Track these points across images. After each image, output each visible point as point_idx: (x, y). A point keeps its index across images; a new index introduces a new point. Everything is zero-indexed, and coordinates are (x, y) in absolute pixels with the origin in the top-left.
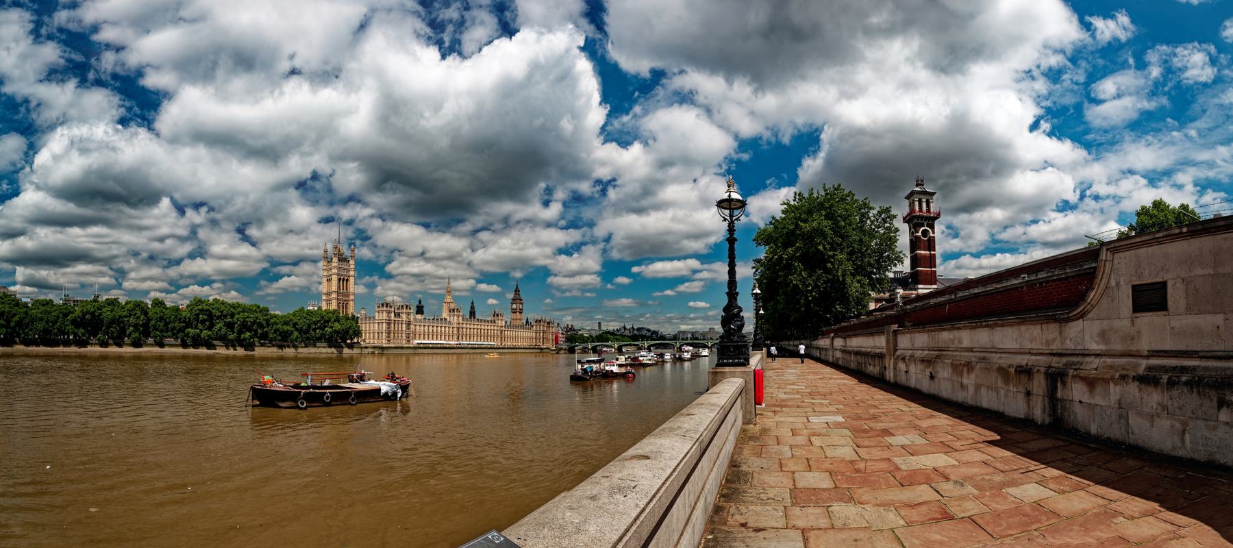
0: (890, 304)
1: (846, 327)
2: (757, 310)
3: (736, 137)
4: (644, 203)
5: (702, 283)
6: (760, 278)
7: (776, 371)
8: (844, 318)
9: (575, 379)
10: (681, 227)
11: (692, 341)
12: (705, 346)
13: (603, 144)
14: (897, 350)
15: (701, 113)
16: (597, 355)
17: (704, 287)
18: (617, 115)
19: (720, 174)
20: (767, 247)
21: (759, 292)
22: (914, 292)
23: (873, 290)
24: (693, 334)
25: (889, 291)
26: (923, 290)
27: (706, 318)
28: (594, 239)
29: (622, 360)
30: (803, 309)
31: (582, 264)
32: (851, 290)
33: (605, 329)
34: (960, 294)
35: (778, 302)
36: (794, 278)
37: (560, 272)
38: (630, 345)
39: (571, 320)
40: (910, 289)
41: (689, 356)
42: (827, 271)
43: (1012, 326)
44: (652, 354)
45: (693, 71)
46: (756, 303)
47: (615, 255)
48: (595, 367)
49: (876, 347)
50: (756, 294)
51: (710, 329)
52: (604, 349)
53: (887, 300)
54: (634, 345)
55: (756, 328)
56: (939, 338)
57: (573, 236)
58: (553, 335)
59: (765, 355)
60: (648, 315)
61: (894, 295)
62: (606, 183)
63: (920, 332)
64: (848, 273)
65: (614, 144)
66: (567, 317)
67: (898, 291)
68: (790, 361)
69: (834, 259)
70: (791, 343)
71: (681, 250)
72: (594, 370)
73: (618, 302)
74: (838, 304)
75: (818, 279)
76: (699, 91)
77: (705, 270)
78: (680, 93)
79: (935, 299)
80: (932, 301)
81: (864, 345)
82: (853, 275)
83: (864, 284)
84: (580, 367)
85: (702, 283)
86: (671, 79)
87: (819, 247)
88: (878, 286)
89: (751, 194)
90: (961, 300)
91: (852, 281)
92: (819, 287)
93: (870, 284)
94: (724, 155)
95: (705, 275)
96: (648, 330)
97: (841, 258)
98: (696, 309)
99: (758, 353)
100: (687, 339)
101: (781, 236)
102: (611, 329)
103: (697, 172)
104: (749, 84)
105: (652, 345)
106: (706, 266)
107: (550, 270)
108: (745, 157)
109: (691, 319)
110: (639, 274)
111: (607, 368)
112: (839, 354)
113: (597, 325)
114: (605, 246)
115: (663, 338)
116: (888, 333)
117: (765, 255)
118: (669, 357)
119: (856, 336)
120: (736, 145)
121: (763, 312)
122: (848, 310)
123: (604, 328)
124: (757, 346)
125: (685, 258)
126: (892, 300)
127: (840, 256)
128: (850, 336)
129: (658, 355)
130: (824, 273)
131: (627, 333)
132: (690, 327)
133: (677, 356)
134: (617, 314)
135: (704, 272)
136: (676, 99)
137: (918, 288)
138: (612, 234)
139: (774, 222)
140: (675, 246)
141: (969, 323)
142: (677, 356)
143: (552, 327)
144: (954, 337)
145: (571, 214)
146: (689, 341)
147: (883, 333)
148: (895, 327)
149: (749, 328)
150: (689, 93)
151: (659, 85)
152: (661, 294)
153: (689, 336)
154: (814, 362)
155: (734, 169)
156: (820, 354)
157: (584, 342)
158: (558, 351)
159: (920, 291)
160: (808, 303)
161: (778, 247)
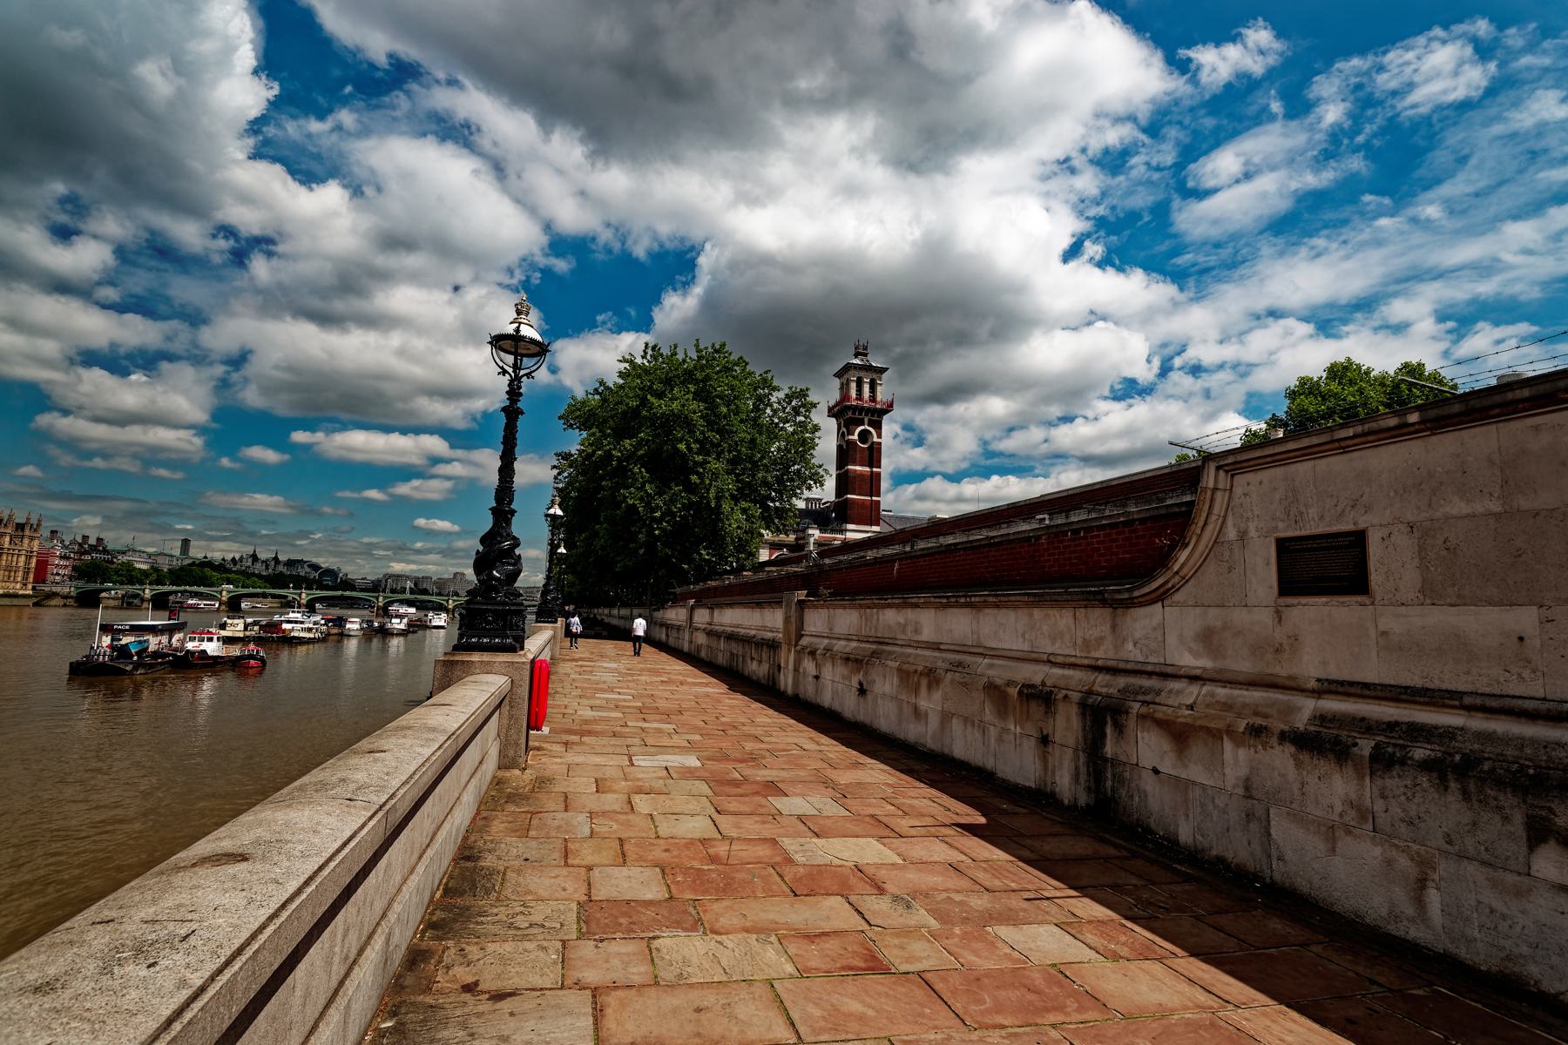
0: (797, 554)
1: (716, 588)
2: (553, 547)
3: (548, 227)
4: (339, 306)
5: (448, 484)
6: (566, 488)
7: (580, 663)
8: (713, 573)
9: (86, 672)
10: (417, 371)
11: (413, 597)
12: (440, 608)
13: (250, 158)
14: (803, 635)
15: (483, 169)
16: (167, 614)
17: (450, 491)
18: (293, 110)
19: (508, 287)
20: (585, 434)
21: (559, 512)
22: (838, 536)
23: (767, 528)
24: (417, 582)
25: (795, 532)
26: (855, 532)
27: (449, 553)
28: (197, 352)
29: (236, 627)
30: (642, 551)
31: (153, 402)
32: (730, 525)
33: (200, 556)
34: (921, 545)
35: (596, 534)
36: (630, 493)
37: (81, 408)
38: (264, 596)
39: (96, 526)
40: (833, 531)
41: (402, 626)
42: (690, 488)
43: (1016, 607)
44: (318, 618)
45: (477, 88)
46: (553, 534)
47: (252, 397)
48: (154, 642)
49: (764, 628)
50: (554, 517)
51: (455, 574)
52: (190, 602)
53: (791, 548)
54: (274, 596)
55: (548, 578)
56: (878, 619)
57: (136, 332)
58: (29, 558)
59: (561, 633)
60: (318, 536)
61: (803, 538)
62: (247, 240)
63: (845, 608)
64: (727, 494)
65: (278, 169)
66: (84, 517)
67: (811, 532)
68: (609, 646)
69: (704, 469)
70: (615, 612)
71: (412, 413)
72: (152, 648)
73: (245, 500)
74: (705, 548)
75: (673, 501)
76: (484, 128)
77: (457, 460)
78: (443, 120)
79: (875, 551)
80: (869, 553)
81: (746, 623)
82: (735, 499)
83: (754, 517)
84: (106, 640)
85: (448, 484)
86: (428, 87)
87: (679, 446)
88: (776, 521)
89: (566, 335)
90: (922, 556)
91: (732, 509)
92: (673, 515)
93: (762, 517)
94: (522, 252)
95: (457, 469)
96: (315, 567)
97: (716, 469)
98: (430, 534)
99: (546, 628)
100: (403, 590)
101: (612, 417)
102: (216, 556)
103: (463, 274)
104: (582, 140)
105: (321, 600)
106: (459, 453)
107: (48, 397)
108: (561, 265)
109: (418, 552)
110: (307, 447)
111: (190, 646)
112: (701, 639)
113: (179, 544)
114: (228, 373)
115: (348, 584)
116: (788, 605)
117: (578, 447)
118: (356, 626)
119: (731, 605)
120: (544, 240)
121: (564, 551)
122: (721, 559)
123: (197, 552)
124: (546, 614)
125: (418, 430)
126: (798, 546)
127: (715, 465)
128: (720, 606)
129: (328, 621)
130: (685, 490)
131: (259, 568)
132: (413, 567)
133: (376, 624)
134: (236, 526)
135: (456, 464)
136: (434, 127)
137: (846, 530)
138: (250, 352)
139: (602, 389)
140: (400, 405)
141: (935, 597)
142: (376, 624)
143: (32, 539)
144: (906, 620)
145: (140, 281)
146: (407, 596)
147: (779, 603)
148: (801, 595)
149: (533, 576)
150: (462, 126)
151: (401, 89)
152: (355, 495)
153: (409, 584)
154: (654, 649)
155: (538, 282)
156: (667, 635)
157: (131, 582)
158: (42, 600)
159: (850, 536)
160: (651, 544)
161: (605, 436)
